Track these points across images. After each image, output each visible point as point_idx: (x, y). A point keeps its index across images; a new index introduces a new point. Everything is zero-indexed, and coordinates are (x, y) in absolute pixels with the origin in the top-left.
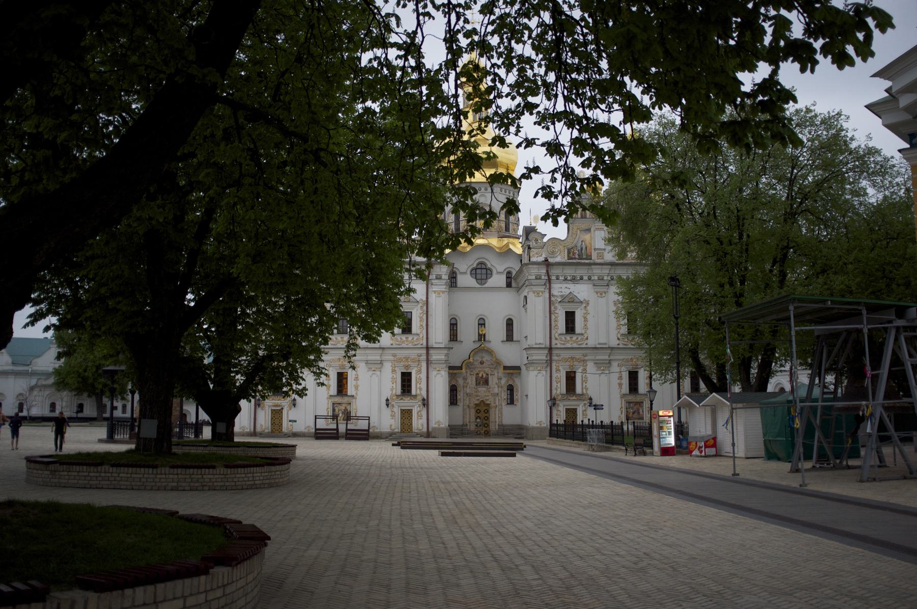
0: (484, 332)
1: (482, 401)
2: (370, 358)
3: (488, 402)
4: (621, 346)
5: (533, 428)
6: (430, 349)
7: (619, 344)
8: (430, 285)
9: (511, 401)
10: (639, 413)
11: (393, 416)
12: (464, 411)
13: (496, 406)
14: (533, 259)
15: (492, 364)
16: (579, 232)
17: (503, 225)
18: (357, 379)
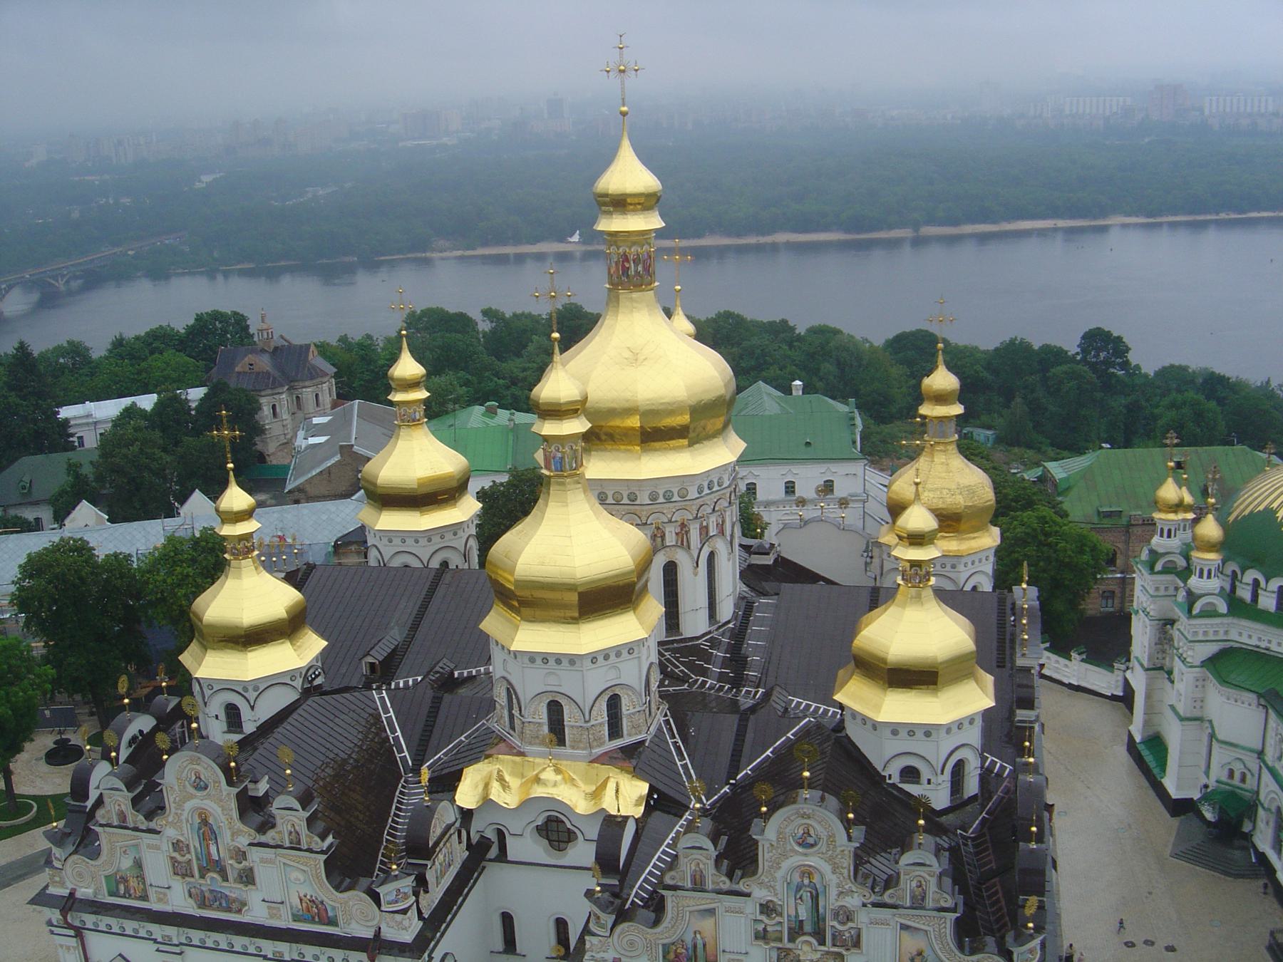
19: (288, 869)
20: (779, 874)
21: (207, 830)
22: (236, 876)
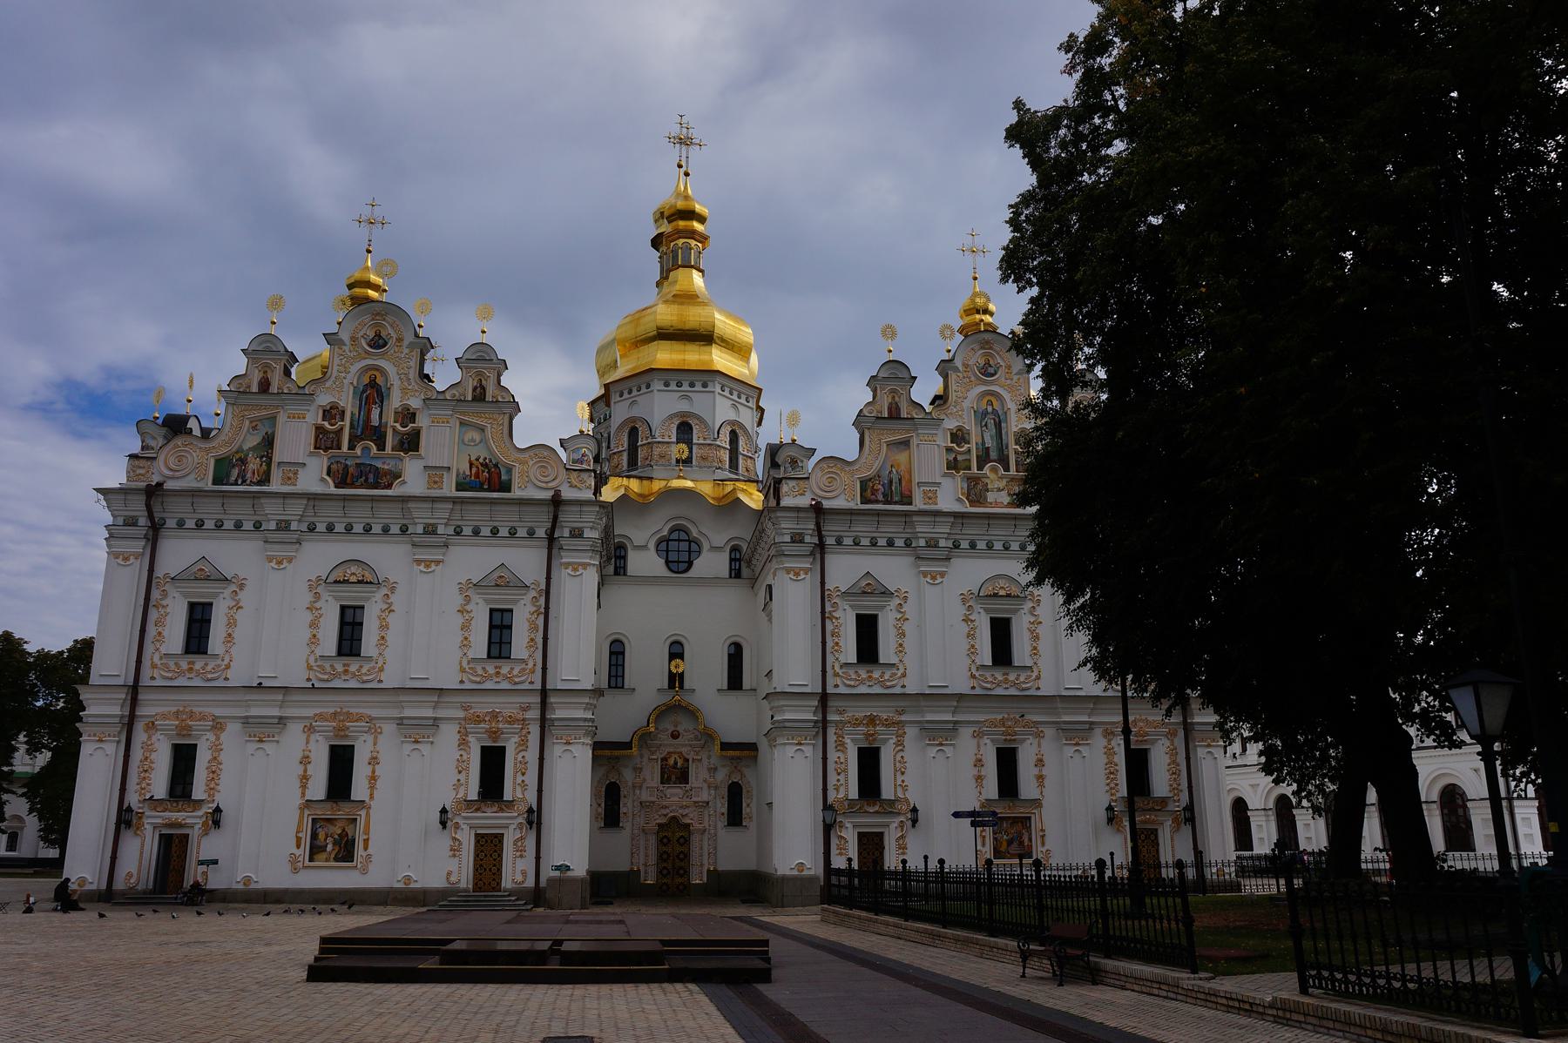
0: (680, 670)
1: (674, 817)
2: (408, 713)
3: (687, 821)
4: (978, 691)
5: (784, 879)
6: (549, 693)
7: (973, 688)
8: (555, 551)
9: (735, 818)
10: (1021, 843)
11: (455, 850)
12: (633, 839)
13: (705, 831)
15: (696, 738)
16: (885, 445)
17: (726, 457)
18: (374, 761)
19: (464, 429)
20: (966, 404)
21: (373, 392)
22: (396, 442)
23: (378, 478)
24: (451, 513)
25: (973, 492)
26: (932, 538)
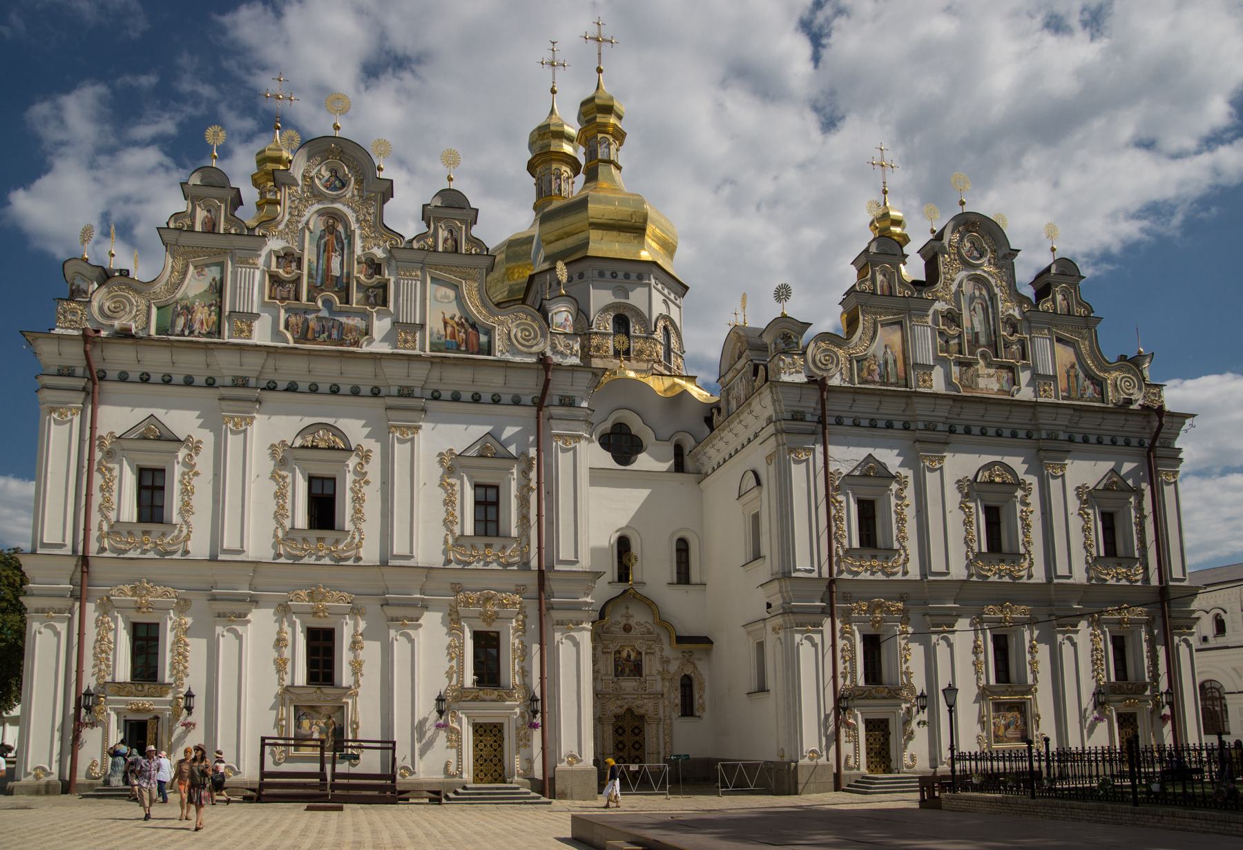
14: (785, 378)
23: (342, 334)
24: (428, 375)
25: (964, 377)
26: (930, 422)
